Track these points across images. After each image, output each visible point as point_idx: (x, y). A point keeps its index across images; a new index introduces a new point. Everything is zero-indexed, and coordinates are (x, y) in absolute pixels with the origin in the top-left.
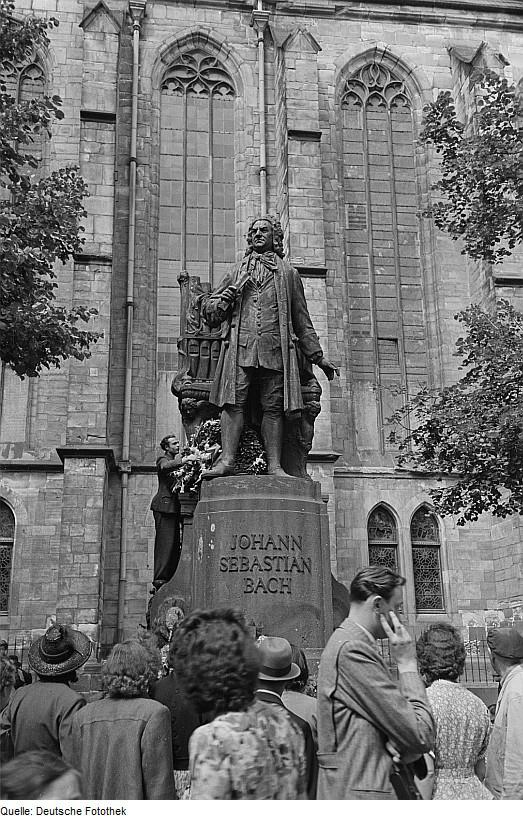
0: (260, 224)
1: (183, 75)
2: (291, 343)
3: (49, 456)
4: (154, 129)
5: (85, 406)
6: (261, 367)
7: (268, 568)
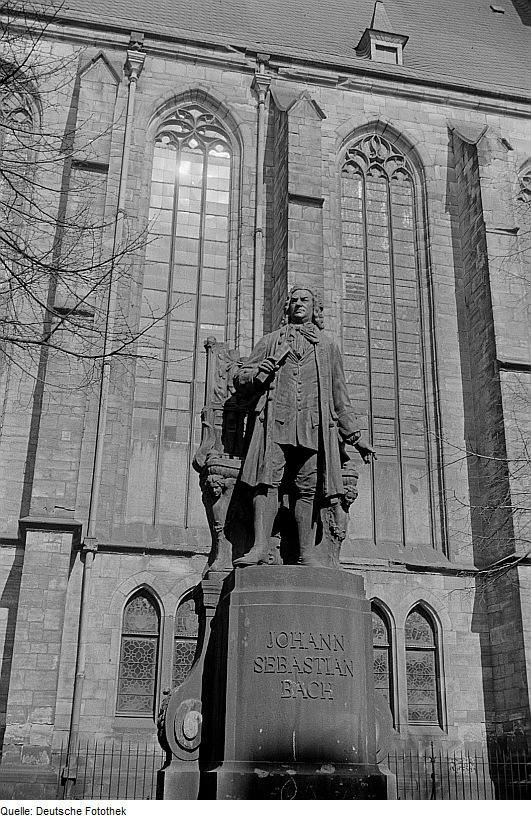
1: (179, 129)
4: (144, 182)
5: (54, 474)
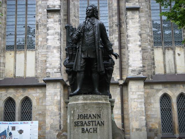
0: (90, 8)
2: (100, 49)
3: (41, 82)
6: (89, 58)
7: (89, 125)
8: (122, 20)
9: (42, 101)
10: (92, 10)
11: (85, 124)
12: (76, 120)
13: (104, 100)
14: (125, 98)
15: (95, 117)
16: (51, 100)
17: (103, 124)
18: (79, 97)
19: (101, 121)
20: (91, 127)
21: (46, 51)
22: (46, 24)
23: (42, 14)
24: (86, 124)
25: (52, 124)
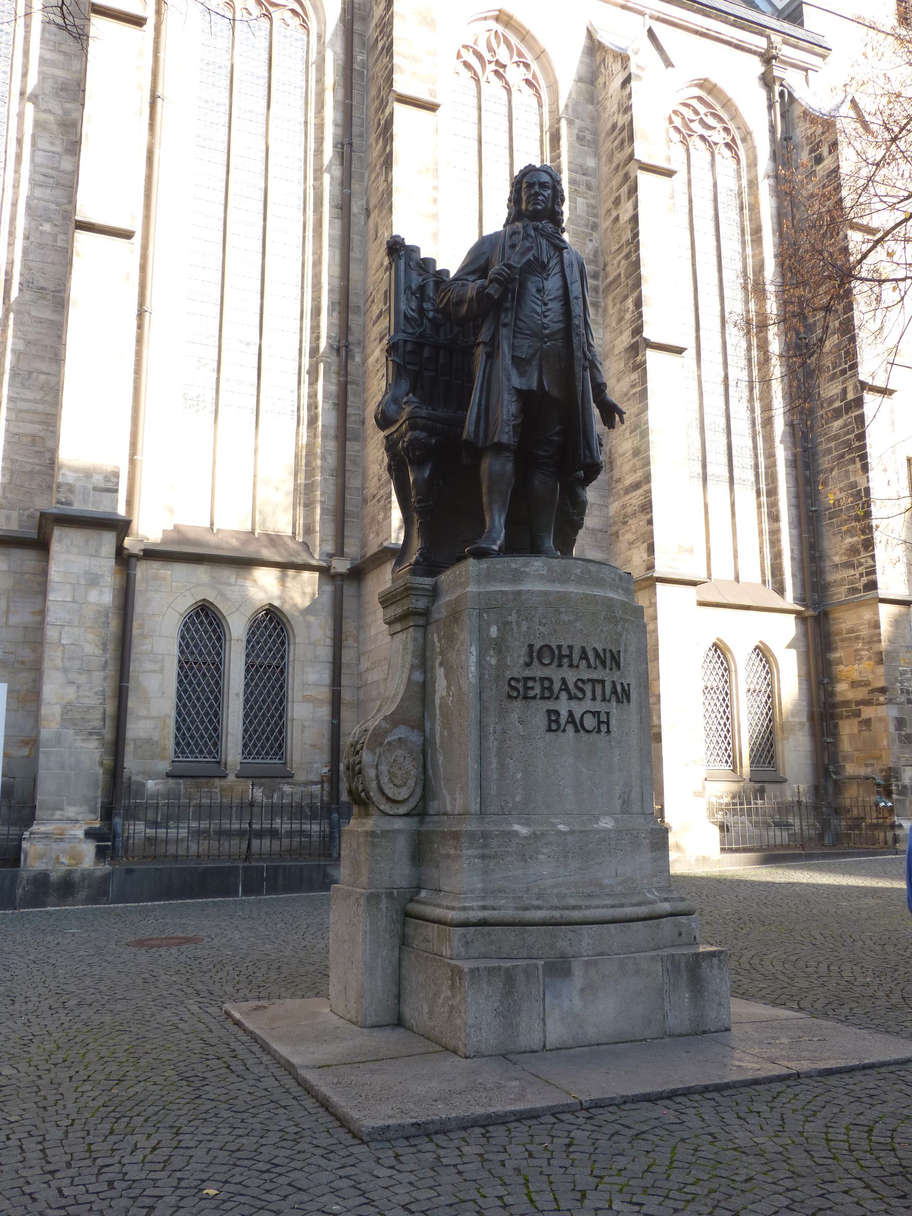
7: (580, 696)
8: (352, 334)
9: (8, 607)
10: (548, 188)
11: (561, 690)
12: (517, 671)
13: (620, 591)
14: (349, 626)
15: (603, 664)
16: (74, 601)
17: (629, 701)
18: (525, 566)
19: (622, 684)
20: (587, 705)
21: (38, 397)
22: (44, 285)
23: (32, 239)
24: (567, 689)
25: (69, 704)
